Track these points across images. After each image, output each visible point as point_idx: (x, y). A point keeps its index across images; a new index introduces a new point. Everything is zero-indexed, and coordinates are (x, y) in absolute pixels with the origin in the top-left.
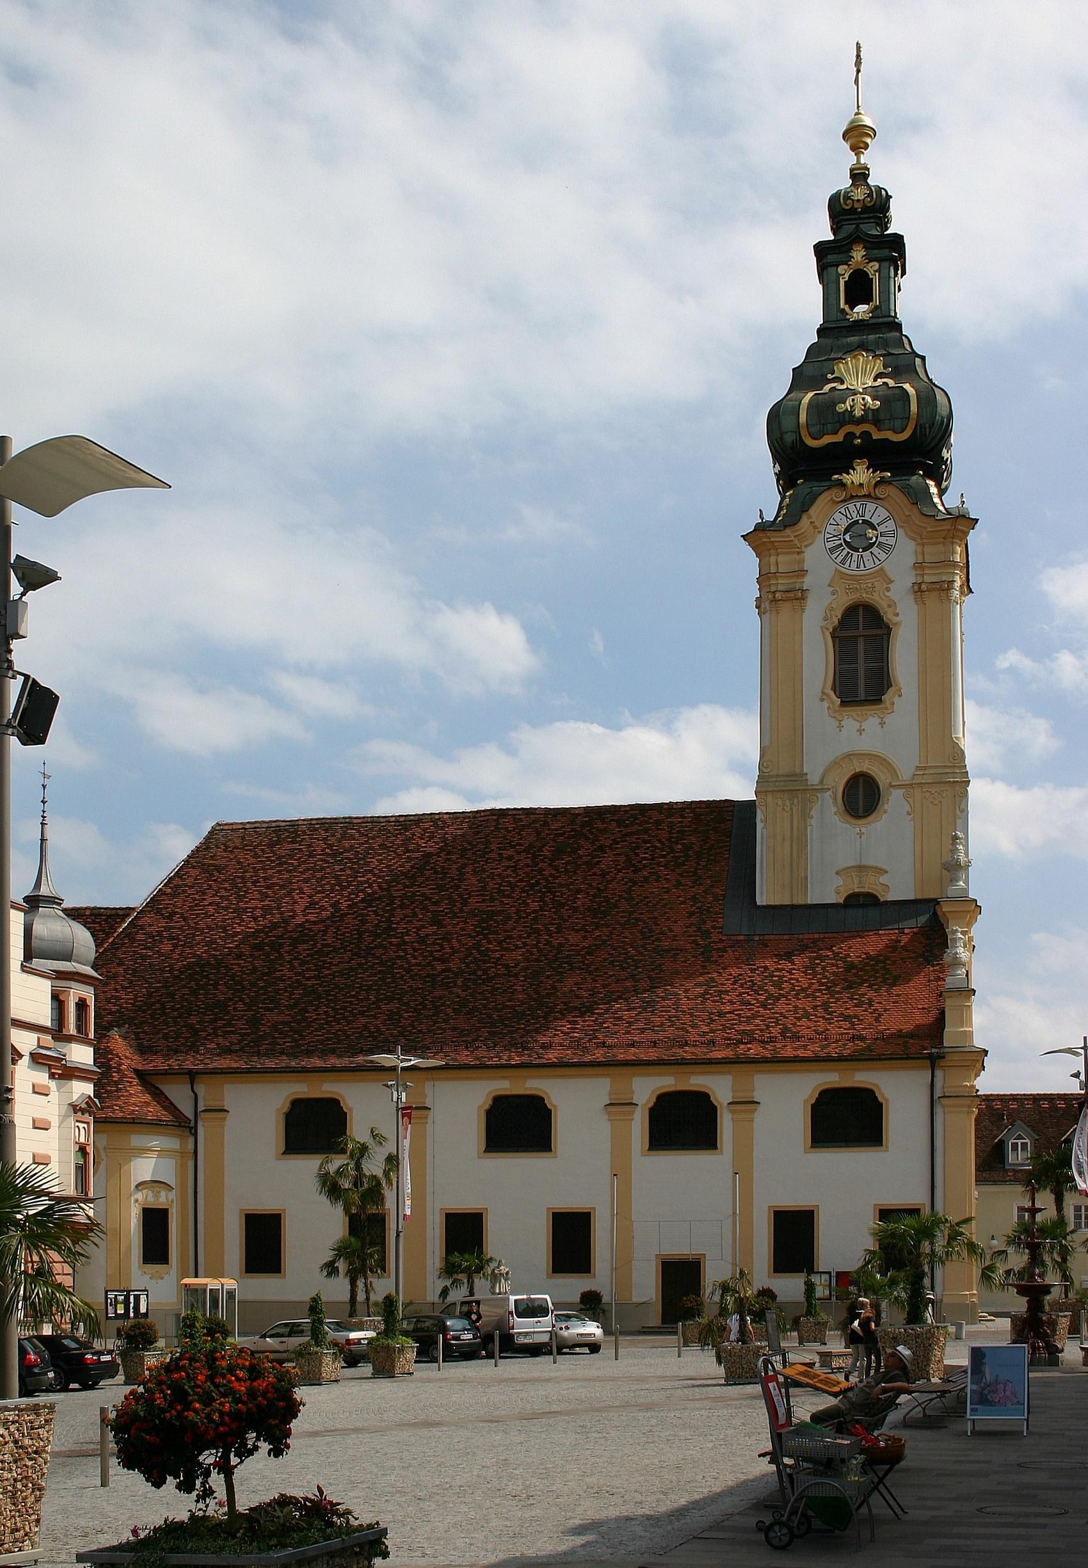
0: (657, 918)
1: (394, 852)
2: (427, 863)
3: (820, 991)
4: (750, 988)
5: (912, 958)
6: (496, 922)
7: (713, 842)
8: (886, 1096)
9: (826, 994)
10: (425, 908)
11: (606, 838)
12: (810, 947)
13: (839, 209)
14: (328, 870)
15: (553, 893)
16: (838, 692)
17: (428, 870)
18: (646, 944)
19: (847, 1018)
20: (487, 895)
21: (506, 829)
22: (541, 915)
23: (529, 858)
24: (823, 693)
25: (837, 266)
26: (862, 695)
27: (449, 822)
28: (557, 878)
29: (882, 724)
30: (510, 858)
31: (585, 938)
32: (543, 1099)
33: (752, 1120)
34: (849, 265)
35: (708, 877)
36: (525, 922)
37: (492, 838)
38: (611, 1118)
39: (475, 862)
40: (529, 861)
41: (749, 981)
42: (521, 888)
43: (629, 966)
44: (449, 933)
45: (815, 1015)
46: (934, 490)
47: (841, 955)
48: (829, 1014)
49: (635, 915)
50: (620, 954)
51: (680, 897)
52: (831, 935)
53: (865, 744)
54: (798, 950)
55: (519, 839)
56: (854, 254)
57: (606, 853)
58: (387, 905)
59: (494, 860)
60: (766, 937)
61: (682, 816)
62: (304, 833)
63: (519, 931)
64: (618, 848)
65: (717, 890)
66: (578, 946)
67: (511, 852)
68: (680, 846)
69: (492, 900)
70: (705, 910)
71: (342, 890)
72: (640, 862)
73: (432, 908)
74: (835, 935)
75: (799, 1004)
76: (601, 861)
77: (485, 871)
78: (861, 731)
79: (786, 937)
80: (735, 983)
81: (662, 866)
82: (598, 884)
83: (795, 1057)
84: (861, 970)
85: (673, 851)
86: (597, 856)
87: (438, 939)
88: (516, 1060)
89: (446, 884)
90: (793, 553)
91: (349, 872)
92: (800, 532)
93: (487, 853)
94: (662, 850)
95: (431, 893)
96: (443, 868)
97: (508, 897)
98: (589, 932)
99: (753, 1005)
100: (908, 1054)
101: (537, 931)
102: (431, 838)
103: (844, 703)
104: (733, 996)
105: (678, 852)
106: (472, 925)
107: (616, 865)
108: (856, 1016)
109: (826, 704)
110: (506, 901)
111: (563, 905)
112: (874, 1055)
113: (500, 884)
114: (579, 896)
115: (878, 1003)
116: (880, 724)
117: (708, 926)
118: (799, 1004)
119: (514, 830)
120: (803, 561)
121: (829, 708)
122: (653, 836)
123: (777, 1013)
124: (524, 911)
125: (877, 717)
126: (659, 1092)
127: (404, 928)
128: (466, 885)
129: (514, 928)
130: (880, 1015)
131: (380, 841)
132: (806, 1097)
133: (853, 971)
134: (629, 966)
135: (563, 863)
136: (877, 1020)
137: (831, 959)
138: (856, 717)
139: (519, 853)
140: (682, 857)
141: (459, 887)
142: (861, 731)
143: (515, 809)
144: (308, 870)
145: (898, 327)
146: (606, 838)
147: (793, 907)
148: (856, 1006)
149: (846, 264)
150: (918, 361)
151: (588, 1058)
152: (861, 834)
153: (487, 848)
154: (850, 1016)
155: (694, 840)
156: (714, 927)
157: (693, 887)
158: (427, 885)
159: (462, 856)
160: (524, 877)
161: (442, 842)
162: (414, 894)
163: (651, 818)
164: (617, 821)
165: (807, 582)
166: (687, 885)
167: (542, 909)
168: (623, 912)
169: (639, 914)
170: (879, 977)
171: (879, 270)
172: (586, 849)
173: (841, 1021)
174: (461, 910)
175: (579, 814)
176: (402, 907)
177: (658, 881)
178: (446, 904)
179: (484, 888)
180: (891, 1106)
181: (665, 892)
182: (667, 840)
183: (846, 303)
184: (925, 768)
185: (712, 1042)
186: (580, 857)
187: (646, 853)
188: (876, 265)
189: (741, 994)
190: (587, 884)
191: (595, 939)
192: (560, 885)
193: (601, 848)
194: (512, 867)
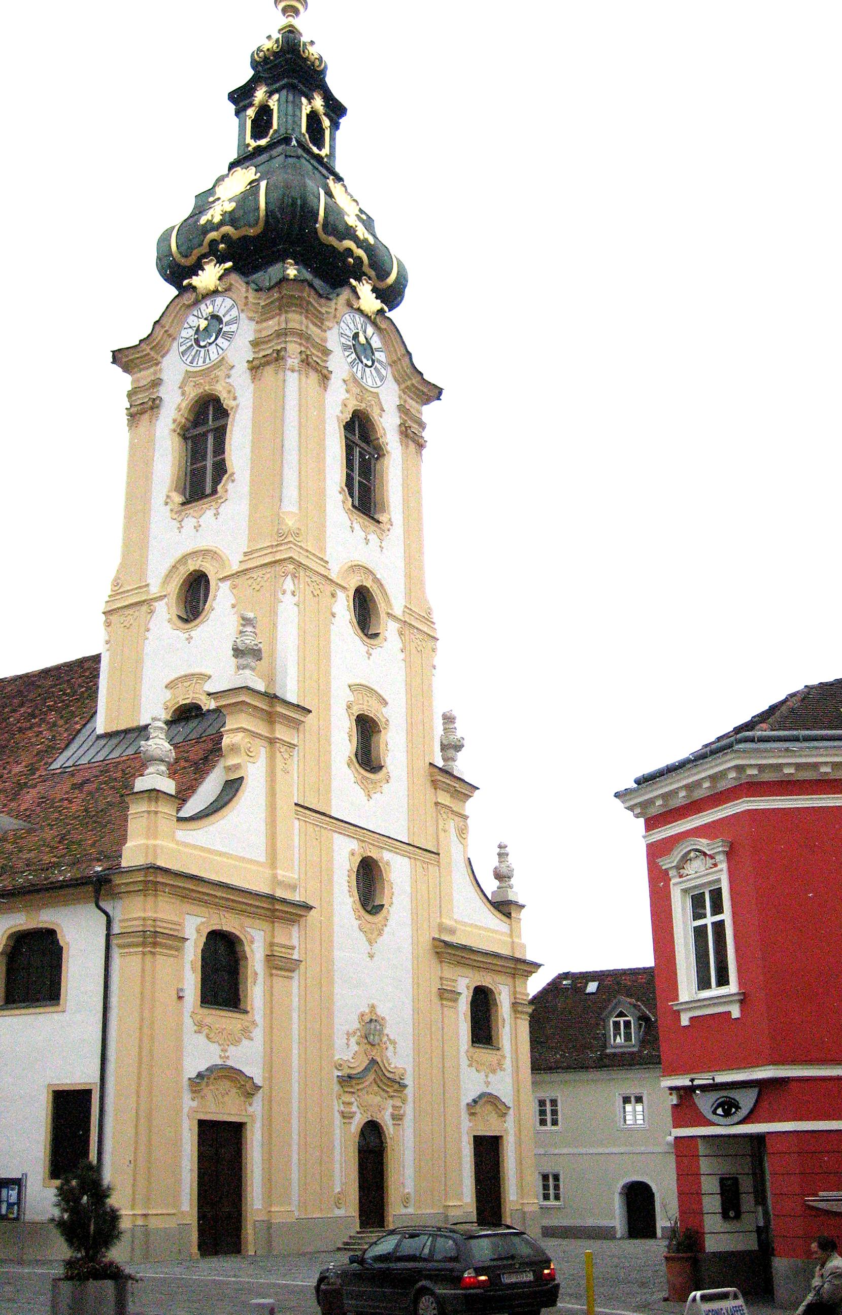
24: (168, 497)
29: (216, 515)
92: (157, 341)
109: (169, 507)
180: (72, 952)
184: (251, 552)
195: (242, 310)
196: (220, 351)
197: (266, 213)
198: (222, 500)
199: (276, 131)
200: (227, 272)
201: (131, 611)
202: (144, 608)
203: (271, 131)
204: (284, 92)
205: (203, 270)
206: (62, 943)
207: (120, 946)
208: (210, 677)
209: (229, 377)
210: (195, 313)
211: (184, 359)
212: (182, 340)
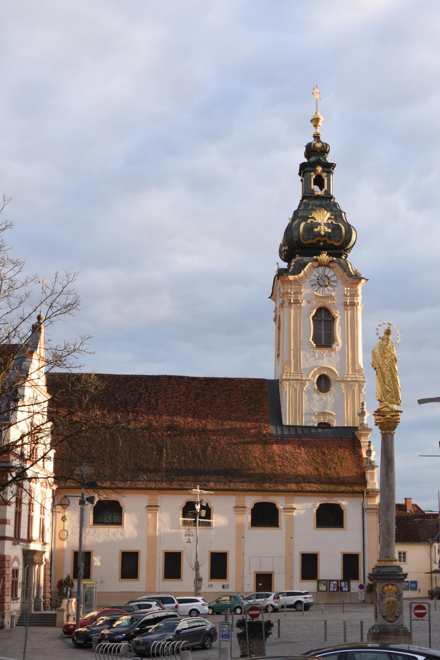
2: (141, 397)
11: (216, 392)
12: (307, 444)
17: (141, 400)
21: (173, 385)
23: (185, 398)
25: (311, 172)
26: (323, 343)
28: (197, 407)
30: (177, 397)
34: (315, 173)
37: (168, 388)
42: (184, 411)
57: (217, 398)
59: (170, 398)
61: (246, 384)
65: (266, 417)
68: (247, 397)
74: (316, 439)
77: (166, 402)
79: (297, 439)
81: (241, 405)
85: (244, 399)
93: (167, 394)
94: (240, 398)
96: (147, 399)
105: (247, 400)
113: (175, 409)
114: (209, 416)
119: (176, 385)
126: (255, 502)
128: (159, 408)
135: (199, 401)
141: (156, 409)
146: (216, 392)
149: (314, 172)
151: (227, 488)
153: (165, 392)
157: (256, 415)
158: (143, 407)
159: (156, 395)
161: (146, 388)
163: (233, 384)
164: (220, 384)
172: (209, 396)
175: (203, 380)
177: (240, 412)
182: (241, 394)
192: (201, 411)
194: (178, 401)
195: (339, 279)
205: (321, 255)
210: (317, 270)
211: (313, 288)
212: (311, 279)
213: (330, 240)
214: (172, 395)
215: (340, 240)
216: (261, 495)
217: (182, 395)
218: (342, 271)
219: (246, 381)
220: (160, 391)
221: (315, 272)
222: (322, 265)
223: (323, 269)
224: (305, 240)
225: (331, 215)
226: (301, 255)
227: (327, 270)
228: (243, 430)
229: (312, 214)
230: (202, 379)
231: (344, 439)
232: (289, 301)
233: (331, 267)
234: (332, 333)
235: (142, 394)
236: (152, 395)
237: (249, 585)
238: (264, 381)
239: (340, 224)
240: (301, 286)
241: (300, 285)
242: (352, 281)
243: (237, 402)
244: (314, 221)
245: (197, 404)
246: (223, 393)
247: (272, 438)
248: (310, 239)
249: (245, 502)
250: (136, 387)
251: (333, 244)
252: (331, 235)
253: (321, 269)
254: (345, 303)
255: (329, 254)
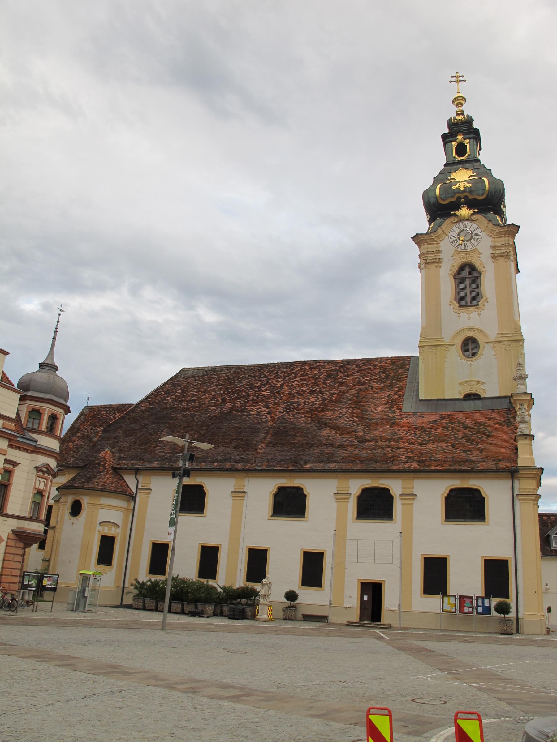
0: (370, 405)
1: (255, 378)
2: (268, 382)
3: (450, 438)
4: (414, 436)
5: (498, 423)
6: (294, 406)
7: (400, 373)
8: (487, 493)
9: (453, 440)
10: (263, 401)
11: (350, 372)
12: (446, 418)
13: (451, 124)
14: (224, 385)
15: (322, 394)
16: (457, 302)
18: (363, 416)
19: (465, 451)
20: (292, 395)
21: (306, 369)
22: (315, 403)
24: (451, 302)
26: (469, 303)
27: (281, 366)
28: (325, 388)
29: (479, 314)
30: (305, 380)
31: (334, 413)
32: (302, 489)
33: (412, 505)
34: (456, 141)
35: (396, 387)
36: (308, 406)
38: (337, 501)
39: (289, 381)
40: (313, 381)
41: (414, 433)
43: (354, 426)
44: (272, 411)
45: (448, 450)
46: (499, 219)
47: (461, 422)
48: (455, 449)
49: (360, 404)
50: (350, 420)
51: (382, 395)
52: (457, 413)
53: (472, 324)
54: (439, 419)
55: (310, 373)
56: (458, 137)
58: (246, 399)
59: (298, 381)
60: (423, 413)
61: (386, 363)
62: (218, 371)
63: (304, 410)
64: (354, 376)
66: (330, 417)
67: (306, 377)
68: (384, 375)
69: (294, 397)
70: (394, 401)
71: (228, 393)
72: (365, 381)
73: (265, 400)
74: (459, 413)
75: (439, 444)
76: (346, 381)
78: (469, 318)
79: (434, 413)
80: (406, 434)
82: (344, 390)
83: (436, 469)
84: (472, 428)
85: (380, 376)
86: (345, 379)
87: (266, 413)
88: (291, 467)
89: (274, 390)
90: (435, 244)
91: (233, 386)
93: (295, 378)
94: (375, 376)
95: (267, 394)
97: (302, 396)
98: (337, 411)
99: (415, 444)
100: (498, 469)
101: (312, 410)
102: (271, 372)
103: (460, 306)
104: (405, 440)
106: (282, 407)
107: (353, 383)
108: (469, 450)
110: (301, 397)
111: (327, 399)
112: (479, 470)
113: (299, 391)
115: (481, 444)
116: (478, 314)
117: (395, 408)
118: (439, 444)
119: (308, 369)
120: (440, 247)
121: (454, 308)
122: (372, 371)
123: (427, 448)
124: (308, 402)
125: (477, 312)
127: (251, 409)
129: (302, 409)
130: (482, 450)
131: (249, 374)
132: (442, 493)
133: (468, 429)
134: (354, 426)
136: (481, 452)
137: (456, 423)
138: (467, 312)
139: (309, 378)
140: (384, 379)
141: (279, 392)
142: (469, 318)
143: (311, 361)
144: (216, 385)
145: (479, 161)
146: (350, 372)
147: (438, 400)
148: (469, 445)
150: (488, 171)
151: (326, 468)
152: (471, 365)
154: (466, 450)
155: (391, 372)
156: (398, 409)
157: (389, 391)
159: (284, 379)
160: (310, 388)
162: (259, 395)
163: (372, 364)
165: (441, 256)
166: (386, 391)
167: (316, 401)
168: (354, 402)
169: (362, 403)
170: (481, 432)
171: (469, 142)
173: (461, 453)
174: (279, 401)
175: (339, 363)
176: (252, 400)
177: (372, 389)
178: (273, 399)
179: (291, 392)
181: (375, 394)
183: (456, 155)
185: (392, 462)
186: (337, 379)
187: (368, 378)
188: (468, 141)
189: (409, 439)
190: (339, 390)
191: (339, 414)
192: (326, 391)
193: (347, 376)
194: (305, 383)
195: (484, 231)
196: (474, 246)
197: (488, 192)
198: (482, 309)
199: (469, 155)
200: (475, 213)
201: (435, 348)
202: (444, 348)
203: (467, 155)
204: (473, 140)
205: (461, 209)
206: (483, 495)
207: (520, 500)
208: (484, 383)
209: (480, 257)
213: (472, 195)
214: (300, 378)
215: (484, 193)
216: (371, 478)
217: (312, 377)
218: (487, 222)
219: (387, 360)
220: (290, 375)
221: (454, 228)
222: (463, 220)
223: (464, 223)
224: (443, 200)
225: (473, 173)
226: (441, 216)
227: (469, 224)
228: (369, 407)
229: (452, 176)
230: (338, 361)
231: (496, 411)
232: (425, 261)
233: (473, 220)
234: (479, 290)
235: (270, 379)
236: (280, 380)
237: (350, 597)
238: (408, 358)
239: (483, 178)
240: (438, 245)
241: (437, 244)
242: (499, 230)
243: (371, 379)
244: (453, 181)
245: (326, 384)
246: (357, 373)
247: (402, 414)
248: (449, 198)
249: (349, 487)
250: (267, 374)
251: (476, 199)
252: (473, 189)
253: (461, 225)
254: (492, 255)
255: (470, 207)
